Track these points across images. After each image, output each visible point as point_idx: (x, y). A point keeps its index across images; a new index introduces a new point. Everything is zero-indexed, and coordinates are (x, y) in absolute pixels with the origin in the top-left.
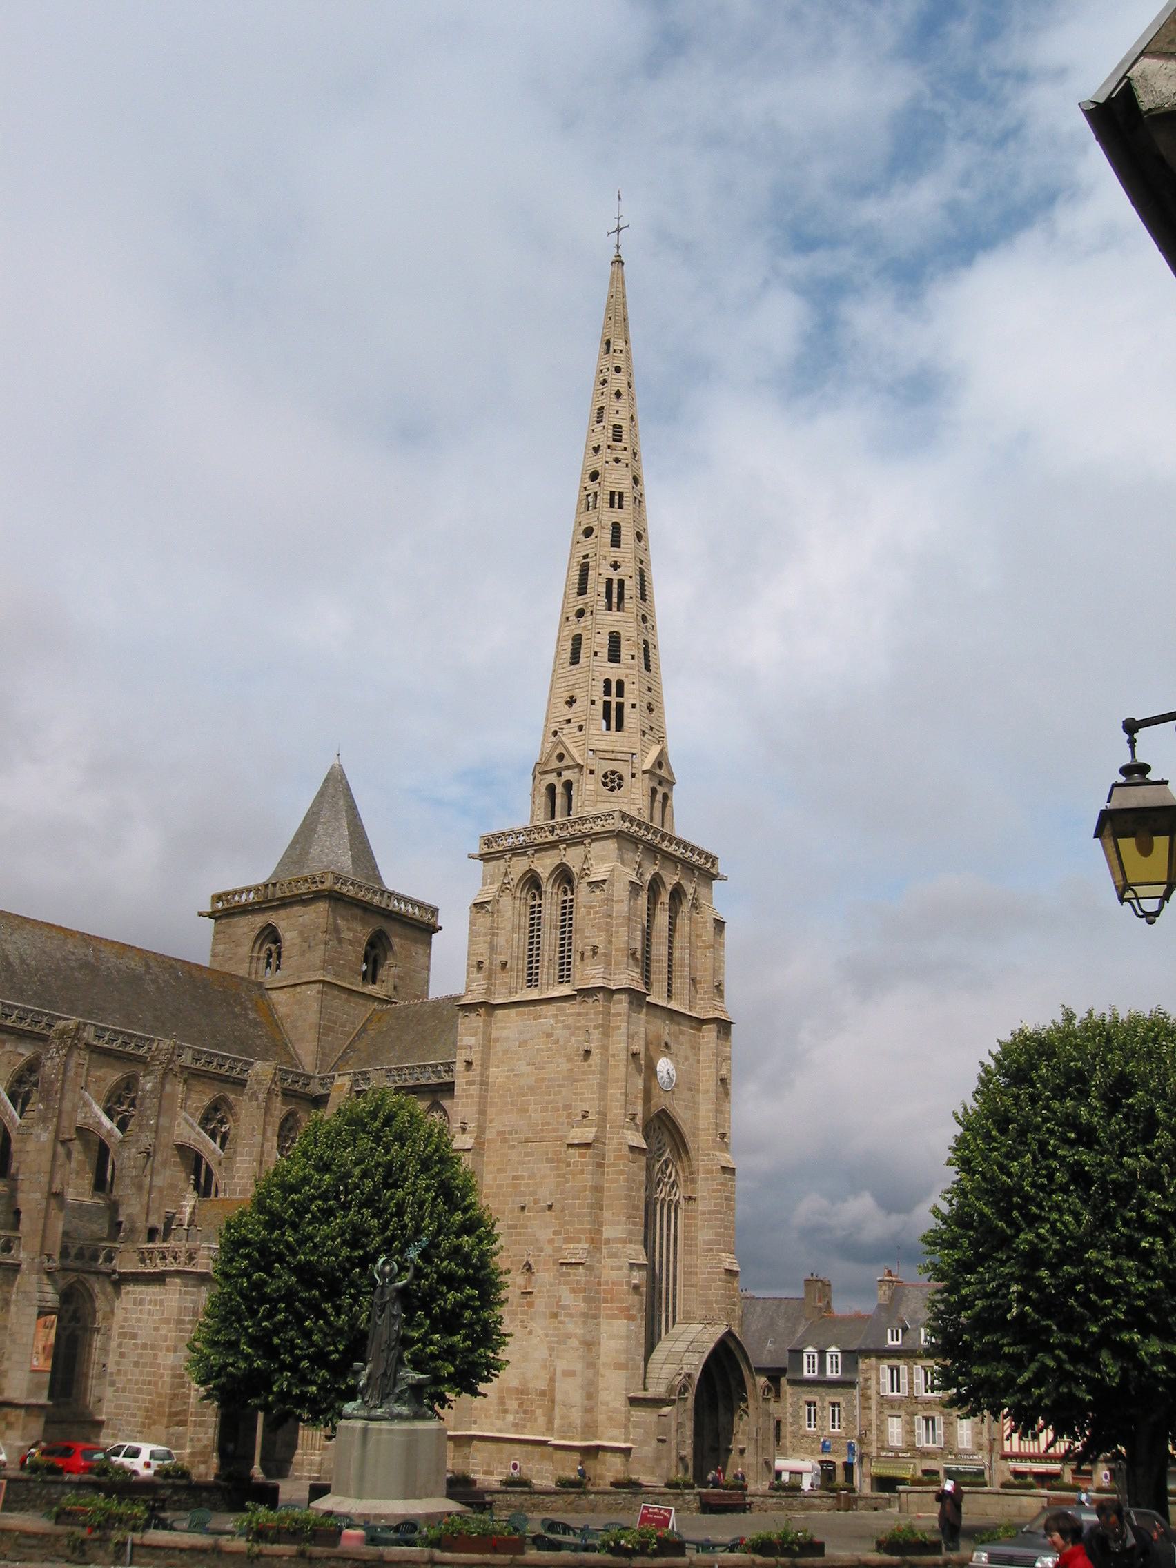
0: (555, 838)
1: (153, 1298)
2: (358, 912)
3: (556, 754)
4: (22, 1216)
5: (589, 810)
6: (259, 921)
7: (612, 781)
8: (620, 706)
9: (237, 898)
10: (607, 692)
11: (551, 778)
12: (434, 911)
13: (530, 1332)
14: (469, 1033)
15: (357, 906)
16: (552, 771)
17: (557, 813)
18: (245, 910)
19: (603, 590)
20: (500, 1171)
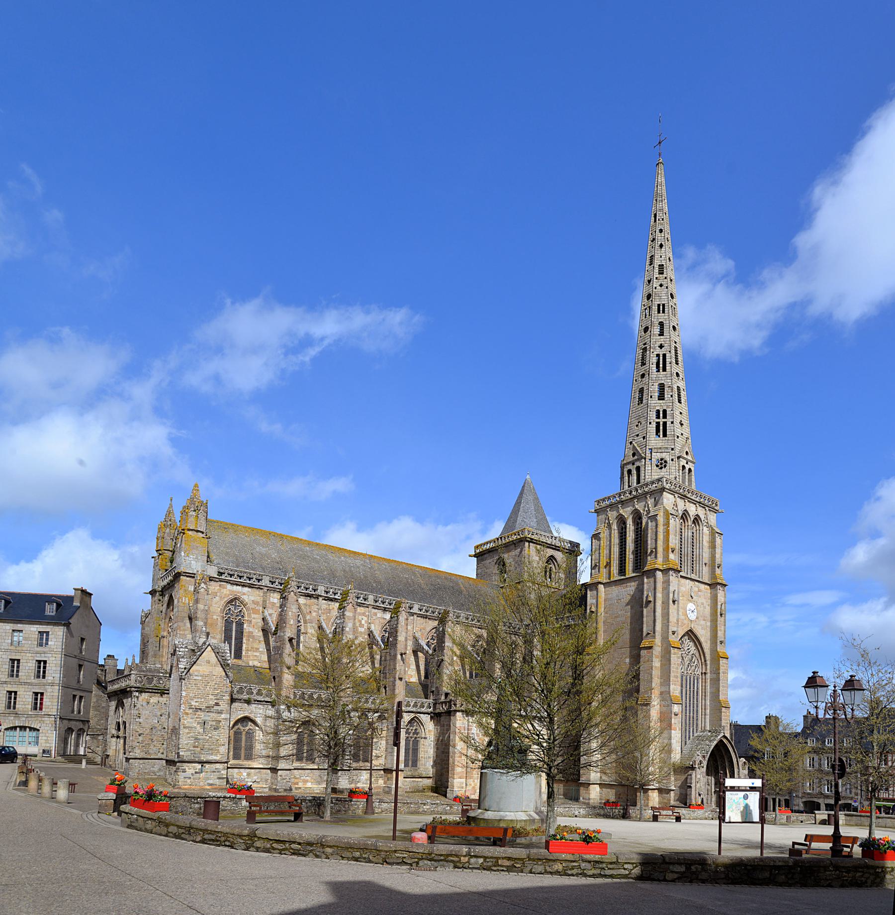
0: (632, 496)
5: (648, 479)
7: (661, 464)
8: (665, 424)
10: (658, 417)
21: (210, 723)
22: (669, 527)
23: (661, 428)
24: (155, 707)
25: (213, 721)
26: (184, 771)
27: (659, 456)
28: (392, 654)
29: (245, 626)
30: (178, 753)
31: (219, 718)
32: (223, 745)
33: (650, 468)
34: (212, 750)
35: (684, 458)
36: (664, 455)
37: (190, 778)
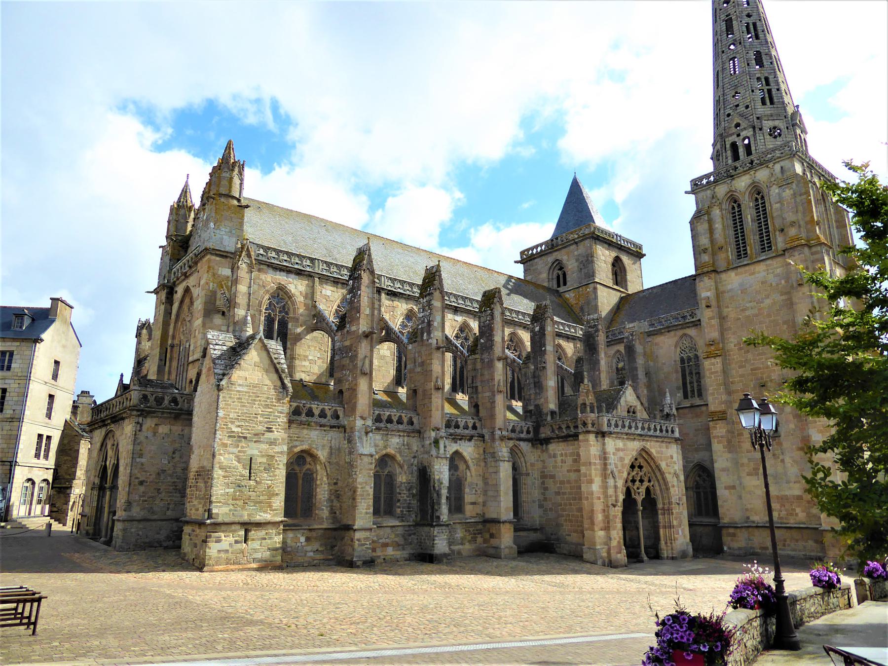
0: (745, 169)
1: (563, 452)
2: (606, 246)
3: (733, 125)
4: (480, 408)
6: (550, 259)
8: (769, 91)
9: (535, 251)
12: (640, 248)
13: (783, 461)
14: (706, 289)
15: (606, 243)
16: (731, 135)
20: (740, 367)
21: (260, 460)
24: (166, 439)
25: (262, 456)
26: (218, 541)
27: (771, 124)
28: (486, 360)
29: (290, 326)
30: (209, 511)
31: (271, 452)
32: (277, 494)
34: (261, 502)
35: (800, 127)
36: (777, 123)
37: (227, 551)
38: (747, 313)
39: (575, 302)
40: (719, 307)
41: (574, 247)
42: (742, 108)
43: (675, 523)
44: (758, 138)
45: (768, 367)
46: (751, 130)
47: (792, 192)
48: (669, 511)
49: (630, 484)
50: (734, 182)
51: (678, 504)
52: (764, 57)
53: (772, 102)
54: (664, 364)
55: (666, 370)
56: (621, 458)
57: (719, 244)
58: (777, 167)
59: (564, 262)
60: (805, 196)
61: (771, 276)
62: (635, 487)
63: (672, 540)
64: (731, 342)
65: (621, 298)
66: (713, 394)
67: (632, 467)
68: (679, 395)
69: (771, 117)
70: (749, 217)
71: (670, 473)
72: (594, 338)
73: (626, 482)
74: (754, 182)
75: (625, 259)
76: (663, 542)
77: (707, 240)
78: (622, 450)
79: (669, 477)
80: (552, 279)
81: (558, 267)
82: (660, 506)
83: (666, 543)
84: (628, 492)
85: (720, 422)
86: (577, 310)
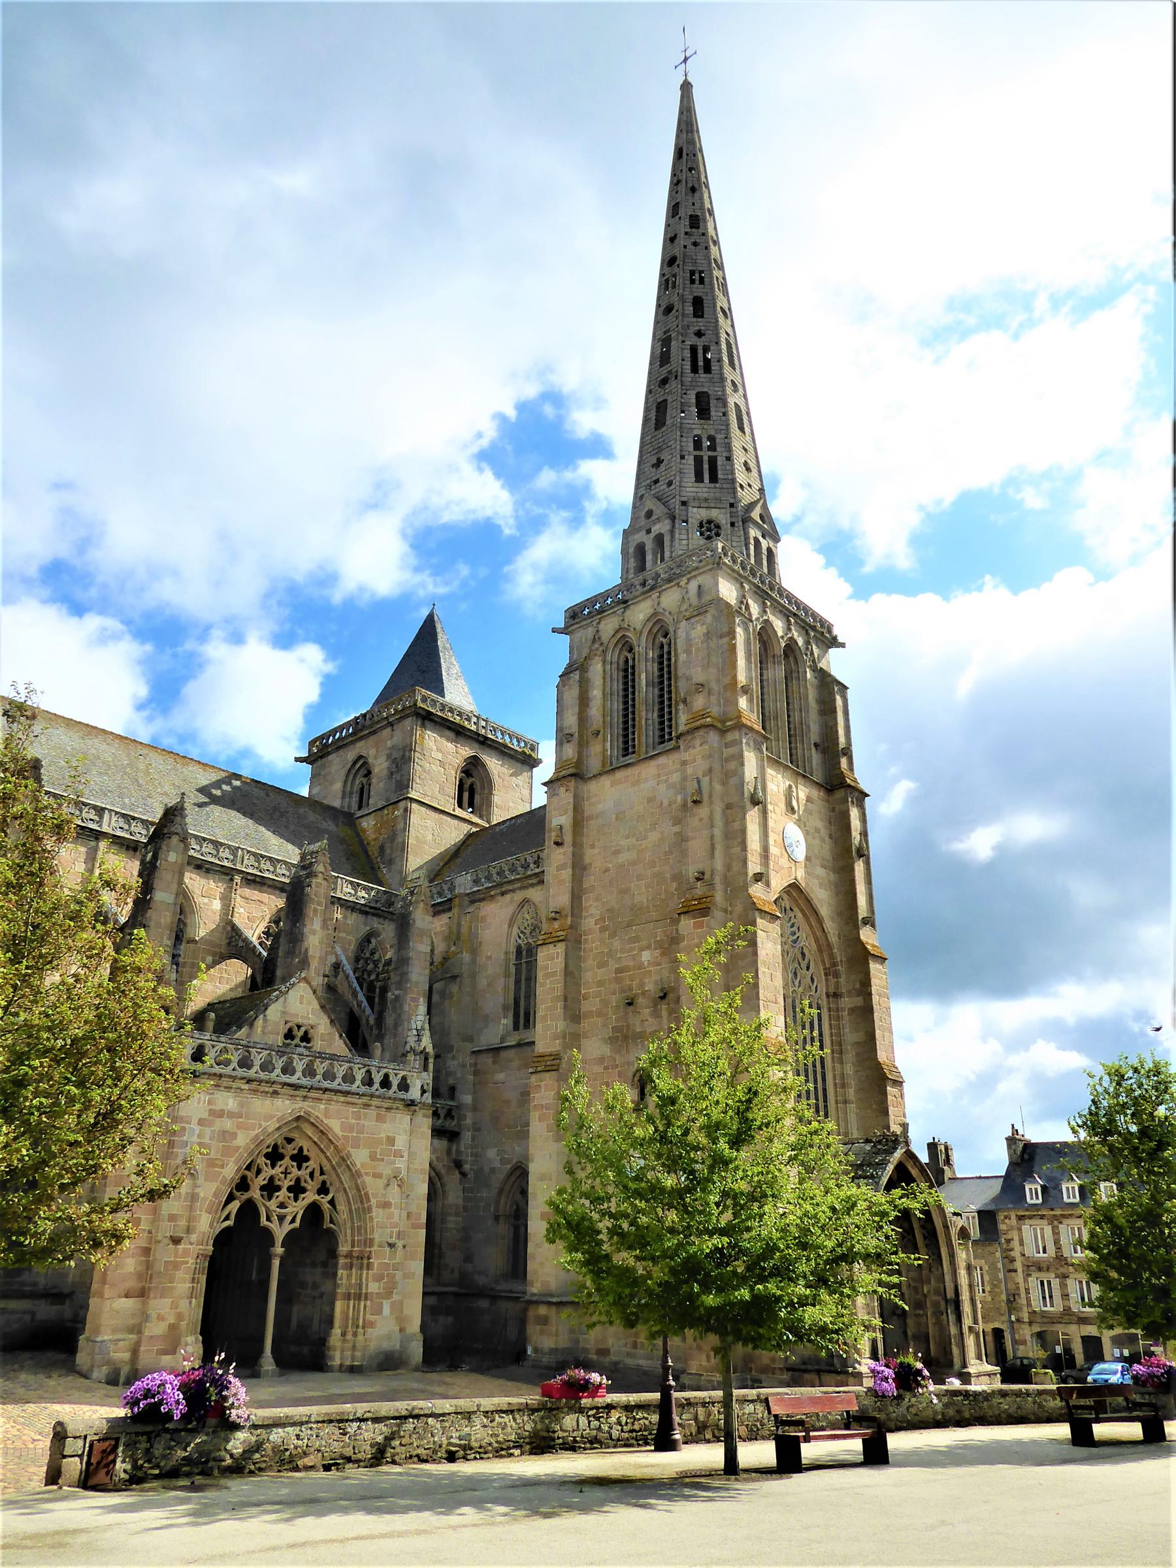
2: (451, 735)
6: (350, 755)
7: (709, 530)
8: (713, 462)
11: (641, 537)
12: (533, 748)
15: (449, 728)
17: (649, 564)
18: (340, 745)
19: (687, 354)
20: (602, 965)
22: (734, 638)
23: (706, 466)
33: (685, 537)
36: (714, 514)
38: (623, 858)
39: (374, 837)
40: (574, 844)
41: (387, 732)
42: (662, 486)
43: (373, 1287)
44: (677, 536)
45: (640, 966)
46: (667, 522)
47: (704, 629)
48: (361, 1260)
49: (255, 1194)
50: (628, 613)
51: (391, 1246)
52: (713, 403)
53: (714, 478)
54: (489, 958)
55: (490, 972)
56: (225, 1132)
57: (595, 727)
58: (693, 586)
59: (370, 760)
60: (725, 640)
61: (663, 787)
62: (273, 1204)
63: (356, 1325)
64: (591, 915)
65: (470, 836)
66: (545, 1017)
67: (274, 1156)
68: (504, 1021)
69: (704, 503)
70: (643, 676)
71: (377, 1176)
72: (303, 888)
73: (243, 1185)
74: (655, 614)
75: (494, 764)
76: (337, 1331)
77: (576, 717)
78: (231, 1115)
79: (373, 1186)
80: (351, 793)
81: (363, 771)
82: (343, 1248)
83: (344, 1334)
84: (249, 1211)
85: (547, 1075)
86: (373, 851)
